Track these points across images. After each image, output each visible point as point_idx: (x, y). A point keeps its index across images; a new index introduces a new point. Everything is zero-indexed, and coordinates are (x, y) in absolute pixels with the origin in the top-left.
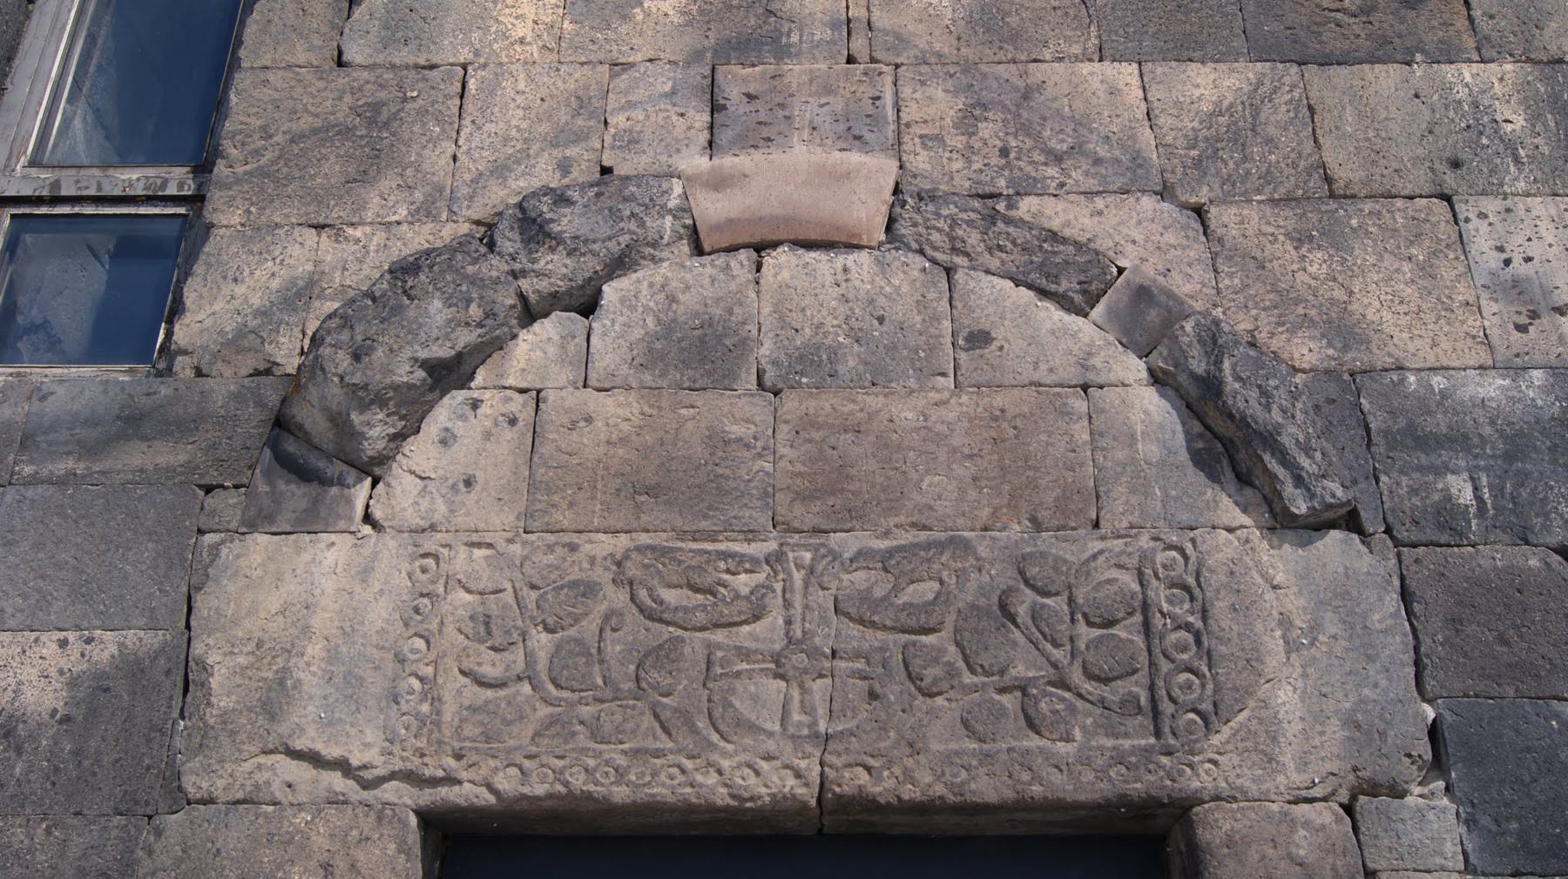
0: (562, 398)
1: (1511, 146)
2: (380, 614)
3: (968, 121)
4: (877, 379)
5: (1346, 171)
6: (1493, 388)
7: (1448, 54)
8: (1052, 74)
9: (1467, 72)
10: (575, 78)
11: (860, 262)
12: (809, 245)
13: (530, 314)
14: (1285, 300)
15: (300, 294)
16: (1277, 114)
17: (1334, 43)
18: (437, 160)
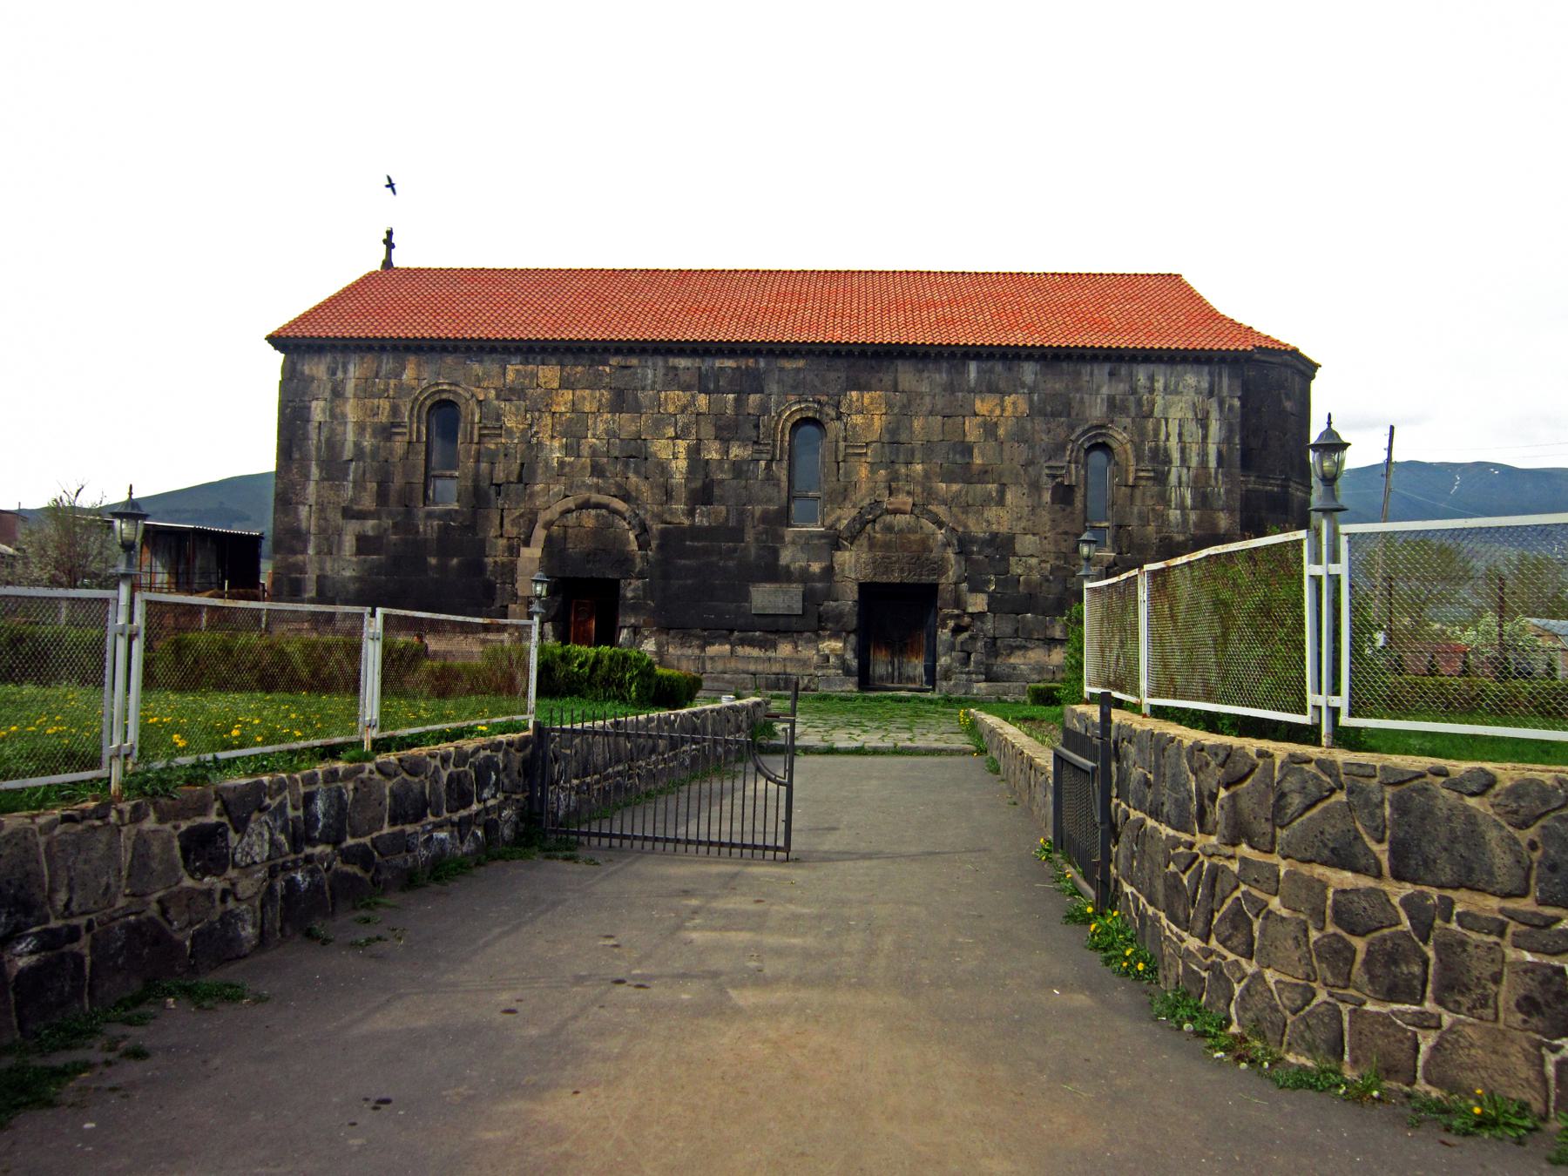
0: (872, 534)
1: (992, 498)
2: (853, 561)
3: (923, 493)
4: (909, 532)
5: (970, 502)
6: (982, 535)
7: (988, 483)
8: (934, 485)
9: (990, 486)
10: (871, 484)
11: (907, 516)
12: (901, 513)
13: (868, 523)
14: (958, 522)
15: (839, 519)
16: (964, 493)
17: (973, 480)
18: (854, 498)
